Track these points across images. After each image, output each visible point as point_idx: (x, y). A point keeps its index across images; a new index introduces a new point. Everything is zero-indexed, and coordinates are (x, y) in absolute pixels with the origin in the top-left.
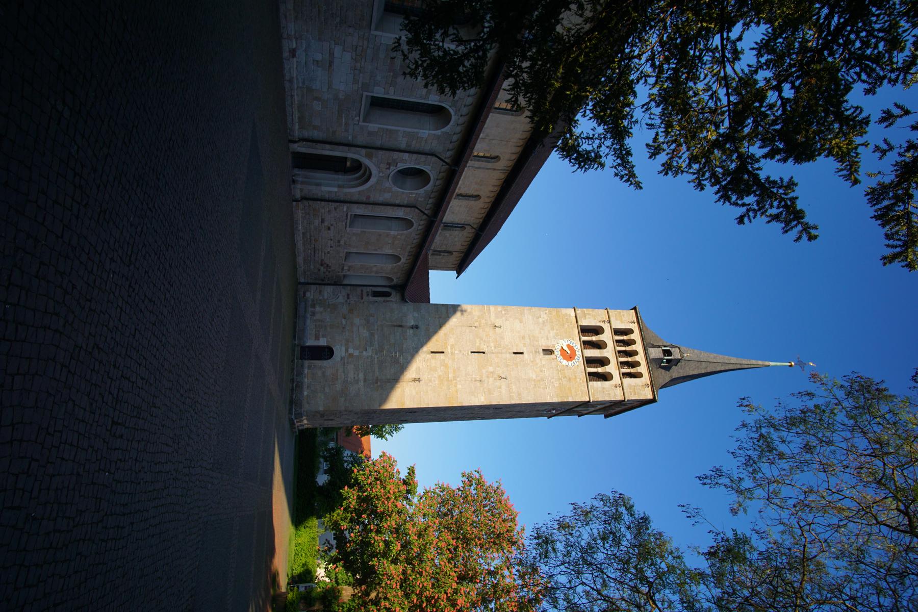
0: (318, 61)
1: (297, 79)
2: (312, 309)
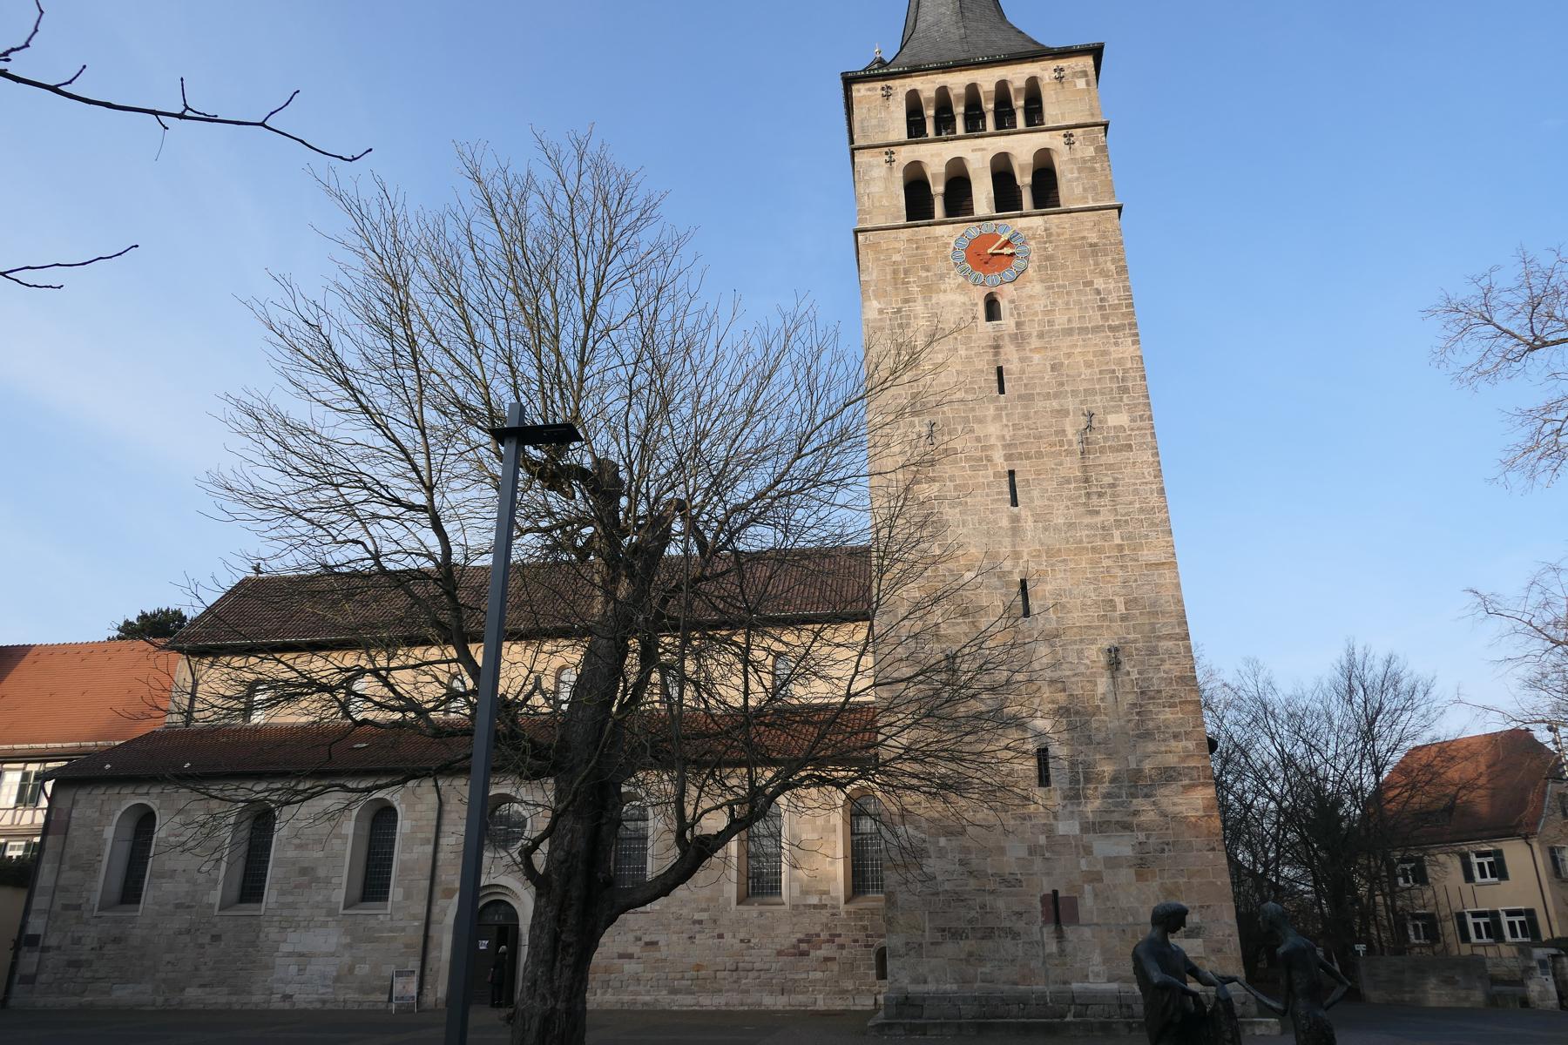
0: (299, 970)
1: (323, 994)
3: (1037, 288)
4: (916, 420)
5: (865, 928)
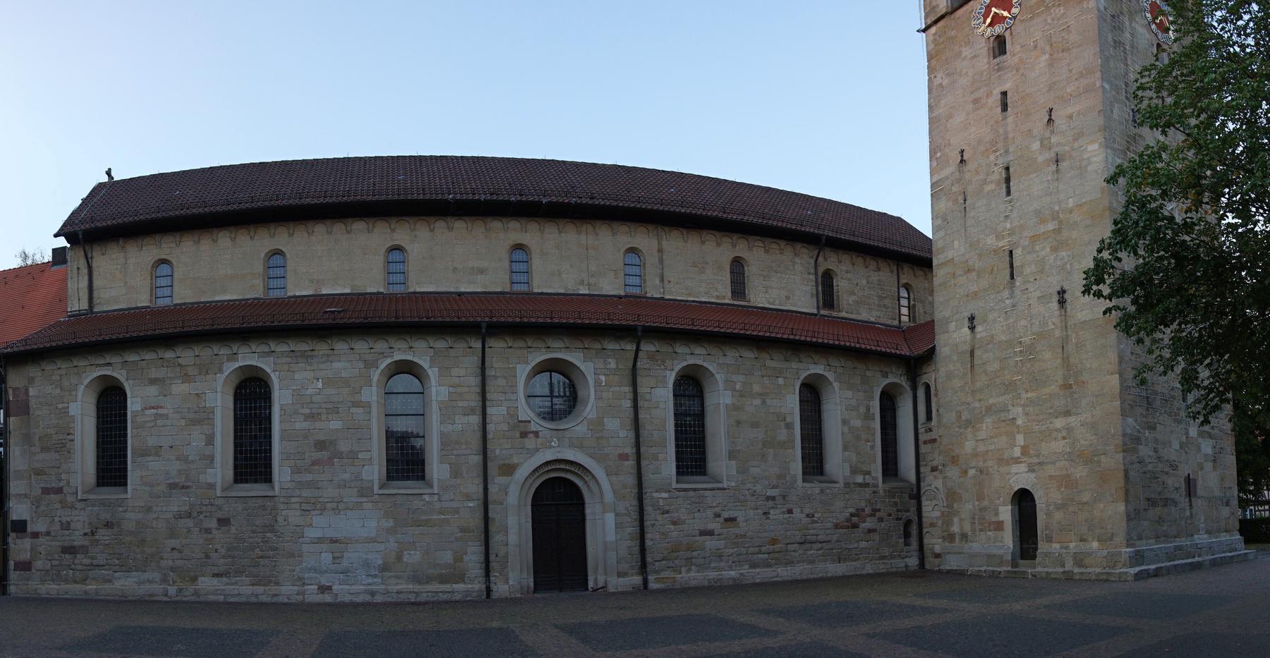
2: (957, 540)
5: (896, 504)
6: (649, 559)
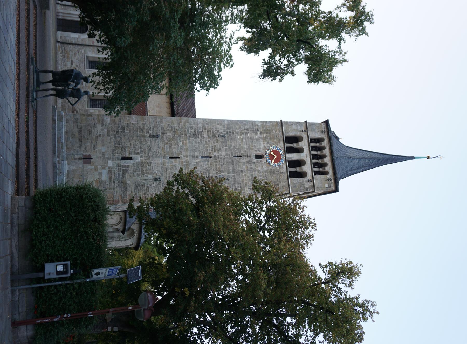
3: (265, 168)
4: (226, 133)
6: (65, 45)
